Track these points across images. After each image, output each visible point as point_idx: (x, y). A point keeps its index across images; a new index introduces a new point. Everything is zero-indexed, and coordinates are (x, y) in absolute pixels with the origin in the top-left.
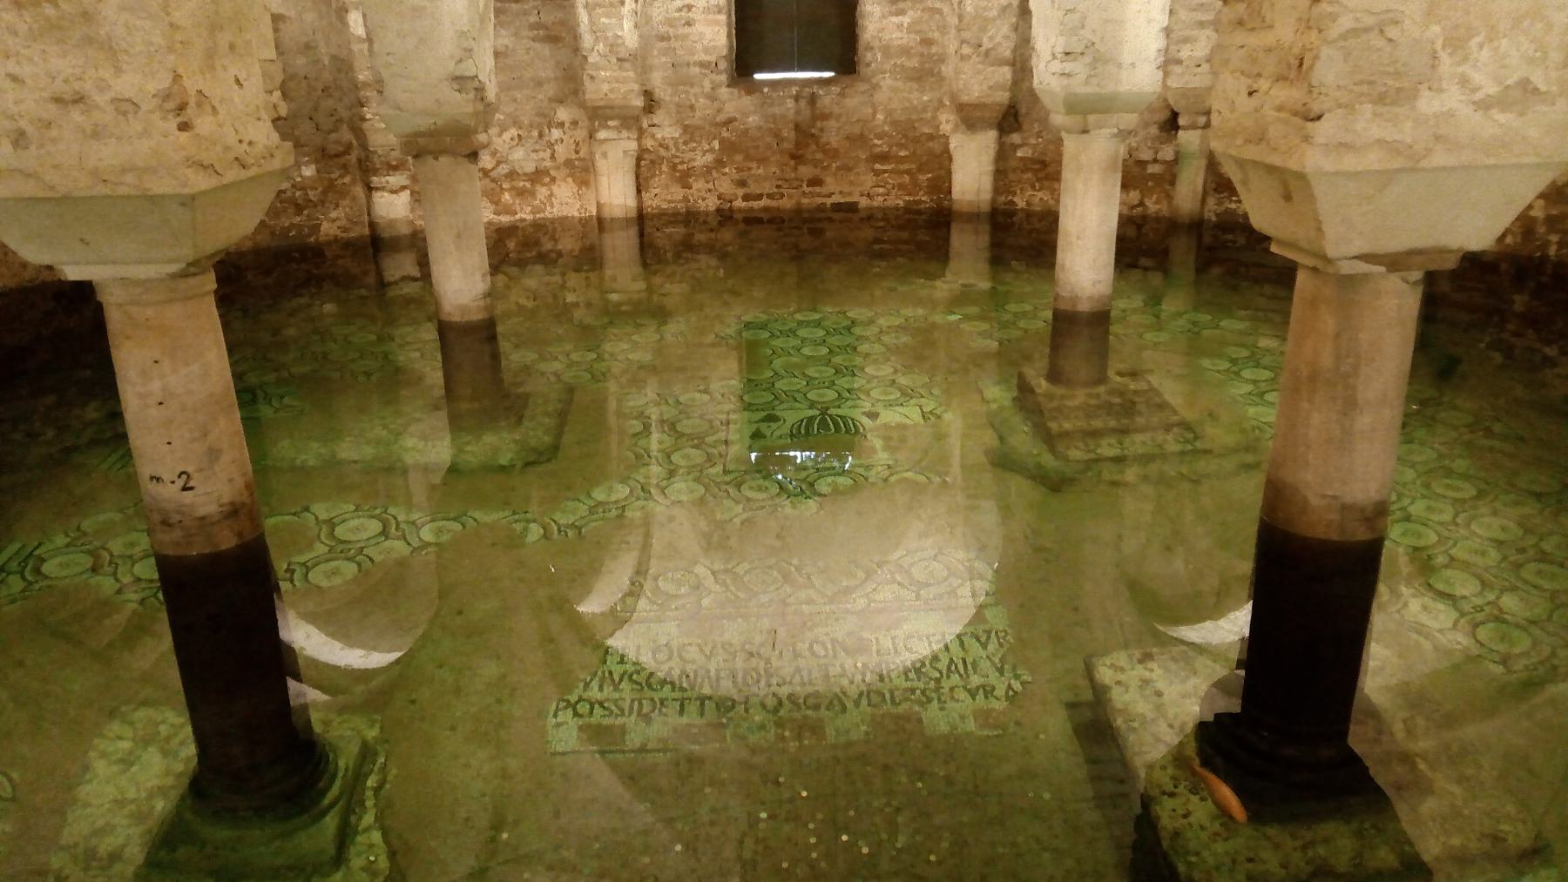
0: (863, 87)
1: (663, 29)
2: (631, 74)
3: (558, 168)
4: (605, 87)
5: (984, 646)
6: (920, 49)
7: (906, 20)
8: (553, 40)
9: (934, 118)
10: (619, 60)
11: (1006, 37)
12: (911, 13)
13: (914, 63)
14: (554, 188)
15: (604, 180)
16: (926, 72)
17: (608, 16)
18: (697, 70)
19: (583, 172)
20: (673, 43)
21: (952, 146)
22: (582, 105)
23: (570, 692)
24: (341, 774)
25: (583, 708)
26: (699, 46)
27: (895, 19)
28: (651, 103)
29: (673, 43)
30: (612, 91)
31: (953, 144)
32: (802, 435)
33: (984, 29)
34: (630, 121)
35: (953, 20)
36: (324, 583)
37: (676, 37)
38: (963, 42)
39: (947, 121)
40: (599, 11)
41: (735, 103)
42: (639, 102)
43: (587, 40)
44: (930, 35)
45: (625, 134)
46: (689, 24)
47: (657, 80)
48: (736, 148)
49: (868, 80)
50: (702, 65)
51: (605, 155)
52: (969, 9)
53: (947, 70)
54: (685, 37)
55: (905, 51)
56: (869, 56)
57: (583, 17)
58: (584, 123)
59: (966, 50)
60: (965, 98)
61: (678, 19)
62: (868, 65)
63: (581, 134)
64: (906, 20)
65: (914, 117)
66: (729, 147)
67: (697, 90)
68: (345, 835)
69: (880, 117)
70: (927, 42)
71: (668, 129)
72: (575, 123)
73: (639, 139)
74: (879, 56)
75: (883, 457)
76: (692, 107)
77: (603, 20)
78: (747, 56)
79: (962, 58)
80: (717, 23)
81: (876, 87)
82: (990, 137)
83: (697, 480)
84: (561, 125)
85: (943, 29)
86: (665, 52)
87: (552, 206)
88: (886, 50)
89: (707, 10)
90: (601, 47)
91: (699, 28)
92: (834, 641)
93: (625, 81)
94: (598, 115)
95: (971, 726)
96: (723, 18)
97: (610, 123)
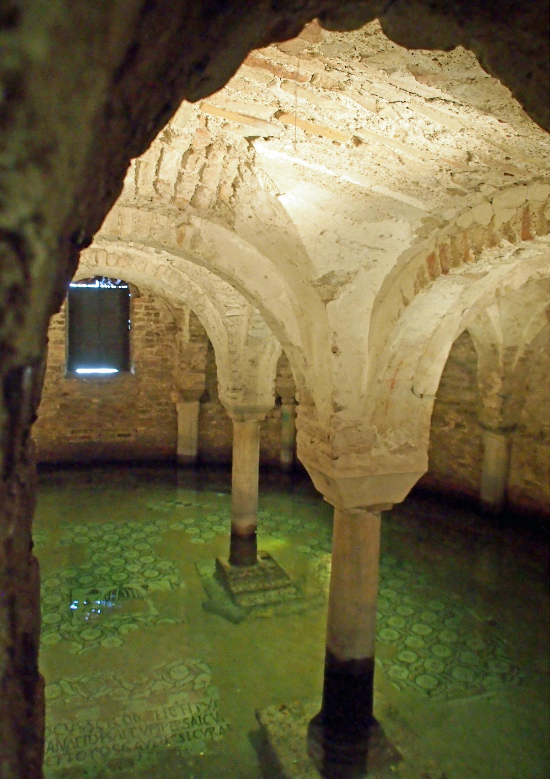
7: (154, 350)
11: (202, 361)
12: (157, 347)
13: (158, 369)
16: (165, 374)
21: (178, 409)
27: (149, 349)
35: (177, 351)
39: (174, 396)
44: (166, 357)
53: (175, 373)
55: (154, 363)
59: (184, 366)
60: (184, 387)
64: (154, 350)
66: (64, 407)
69: (142, 393)
70: (165, 360)
74: (141, 365)
79: (182, 369)
80: (60, 348)
82: (196, 404)
85: (172, 354)
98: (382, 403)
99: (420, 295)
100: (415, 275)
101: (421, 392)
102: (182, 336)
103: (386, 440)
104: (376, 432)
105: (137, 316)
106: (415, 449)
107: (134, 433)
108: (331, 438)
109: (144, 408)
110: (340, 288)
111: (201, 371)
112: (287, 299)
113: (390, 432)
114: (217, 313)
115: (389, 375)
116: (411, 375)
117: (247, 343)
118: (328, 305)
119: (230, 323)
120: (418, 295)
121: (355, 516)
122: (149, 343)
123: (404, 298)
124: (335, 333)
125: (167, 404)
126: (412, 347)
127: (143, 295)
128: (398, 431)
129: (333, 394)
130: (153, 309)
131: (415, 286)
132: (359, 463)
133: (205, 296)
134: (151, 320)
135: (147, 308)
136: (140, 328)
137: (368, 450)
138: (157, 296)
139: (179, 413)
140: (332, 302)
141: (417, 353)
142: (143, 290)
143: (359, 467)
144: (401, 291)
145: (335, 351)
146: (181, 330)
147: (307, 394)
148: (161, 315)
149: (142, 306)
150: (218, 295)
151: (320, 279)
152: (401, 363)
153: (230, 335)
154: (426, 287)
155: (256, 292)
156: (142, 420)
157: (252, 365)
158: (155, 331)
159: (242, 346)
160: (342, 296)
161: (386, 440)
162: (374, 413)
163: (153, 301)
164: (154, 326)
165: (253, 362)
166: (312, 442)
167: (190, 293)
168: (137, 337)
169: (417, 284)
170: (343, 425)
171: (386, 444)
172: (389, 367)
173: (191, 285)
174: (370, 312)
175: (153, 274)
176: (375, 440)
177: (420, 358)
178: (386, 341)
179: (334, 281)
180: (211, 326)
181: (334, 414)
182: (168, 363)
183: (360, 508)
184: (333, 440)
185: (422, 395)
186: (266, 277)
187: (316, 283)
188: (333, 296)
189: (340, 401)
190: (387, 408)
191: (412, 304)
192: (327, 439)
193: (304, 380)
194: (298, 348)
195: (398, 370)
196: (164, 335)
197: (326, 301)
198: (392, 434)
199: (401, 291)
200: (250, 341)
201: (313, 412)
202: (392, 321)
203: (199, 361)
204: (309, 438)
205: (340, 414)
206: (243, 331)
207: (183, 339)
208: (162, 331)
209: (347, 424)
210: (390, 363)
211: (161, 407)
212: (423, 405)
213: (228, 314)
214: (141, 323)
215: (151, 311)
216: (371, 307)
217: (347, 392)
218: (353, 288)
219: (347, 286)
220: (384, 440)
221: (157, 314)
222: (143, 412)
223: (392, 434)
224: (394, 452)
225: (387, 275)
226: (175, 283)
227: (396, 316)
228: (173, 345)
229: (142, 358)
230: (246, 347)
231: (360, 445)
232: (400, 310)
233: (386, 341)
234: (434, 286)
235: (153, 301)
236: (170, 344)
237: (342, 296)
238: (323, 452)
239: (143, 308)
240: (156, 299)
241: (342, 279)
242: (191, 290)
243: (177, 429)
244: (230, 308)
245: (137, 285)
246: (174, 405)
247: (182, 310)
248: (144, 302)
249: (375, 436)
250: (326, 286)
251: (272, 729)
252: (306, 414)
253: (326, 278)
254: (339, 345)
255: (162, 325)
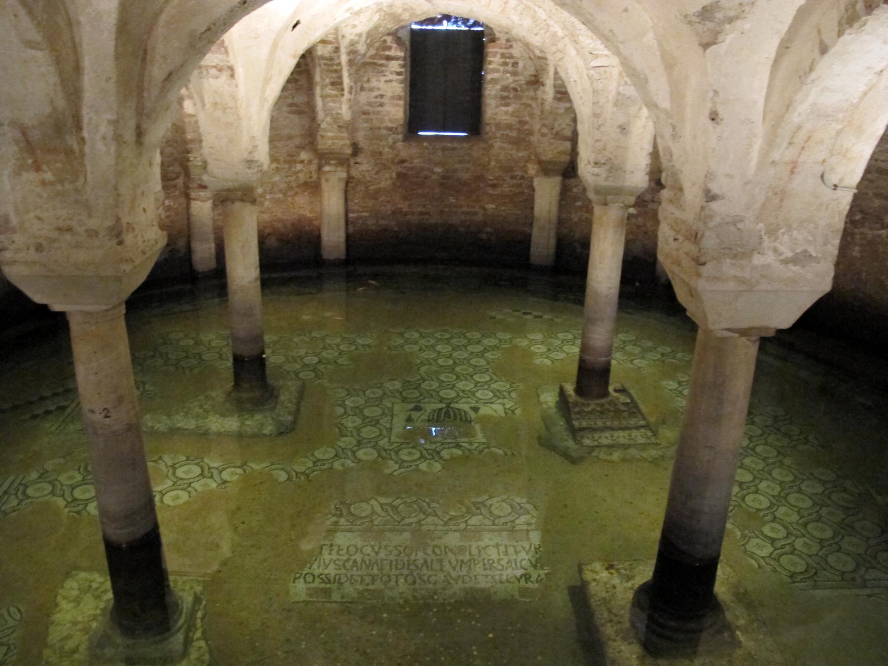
0: (482, 145)
1: (366, 108)
2: (346, 135)
3: (298, 187)
4: (330, 142)
5: (527, 553)
6: (517, 126)
7: (510, 109)
8: (300, 113)
9: (525, 166)
10: (339, 127)
12: (513, 105)
13: (514, 134)
14: (296, 198)
15: (325, 195)
17: (334, 102)
18: (384, 132)
19: (314, 188)
20: (372, 116)
22: (315, 151)
23: (303, 570)
24: (185, 611)
25: (309, 578)
26: (387, 118)
27: (503, 108)
28: (356, 149)
29: (372, 116)
30: (333, 144)
31: (536, 182)
32: (436, 418)
33: (555, 120)
34: (343, 162)
35: (537, 112)
36: (171, 503)
37: (374, 113)
38: (543, 125)
39: (532, 169)
40: (329, 99)
41: (406, 151)
42: (349, 151)
43: (321, 115)
45: (339, 169)
46: (381, 105)
47: (360, 137)
48: (408, 180)
49: (486, 143)
50: (389, 129)
51: (327, 180)
52: (547, 108)
53: (534, 139)
54: (379, 113)
55: (509, 127)
56: (488, 129)
57: (319, 102)
58: (315, 161)
59: (545, 130)
60: (543, 158)
61: (376, 102)
62: (487, 133)
63: (314, 167)
64: (510, 109)
65: (513, 165)
66: (401, 176)
67: (384, 143)
68: (188, 642)
69: (493, 163)
70: (522, 123)
71: (366, 165)
72: (310, 162)
73: (348, 172)
74: (494, 129)
75: (480, 437)
76: (380, 153)
77: (332, 104)
78: (415, 121)
79: (543, 135)
80: (398, 105)
81: (492, 146)
83: (374, 447)
84: (302, 162)
85: (532, 115)
86: (367, 121)
87: (294, 208)
88: (498, 126)
89: (393, 98)
90: (328, 119)
91: (387, 108)
92: (445, 547)
93: (342, 138)
94: (323, 157)
95: (517, 595)
96: (402, 102)
97: (332, 162)
98: (776, 194)
99: (846, 37)
100: (842, 8)
101: (835, 182)
102: (544, 92)
103: (776, 244)
104: (763, 233)
105: (490, 67)
106: (816, 260)
107: (481, 212)
108: (699, 236)
109: (495, 182)
110: (727, 26)
111: (566, 139)
112: (655, 41)
113: (783, 234)
114: (581, 63)
115: (789, 155)
116: (821, 157)
117: (616, 104)
118: (707, 51)
119: (596, 76)
120: (842, 39)
121: (723, 340)
122: (504, 100)
123: (821, 42)
124: (715, 92)
125: (522, 177)
126: (828, 116)
127: (499, 39)
128: (795, 233)
129: (706, 176)
130: (511, 57)
131: (840, 24)
132: (732, 272)
133: (567, 39)
134: (507, 72)
135: (503, 56)
136: (495, 81)
137: (747, 255)
138: (515, 40)
139: (537, 188)
140: (715, 46)
141: (834, 125)
142: (500, 32)
143: (735, 276)
144: (819, 32)
145: (714, 117)
146: (543, 84)
147: (675, 175)
148: (521, 65)
149: (497, 52)
150: (581, 39)
151: (698, 12)
152: (809, 138)
153: (595, 92)
154: (856, 25)
155: (611, 31)
156: (491, 195)
157: (621, 133)
158: (512, 86)
159: (610, 108)
160: (729, 38)
161: (776, 244)
162: (763, 206)
163: (511, 46)
164: (511, 79)
165: (623, 129)
166: (675, 240)
167: (547, 35)
168: (491, 92)
169: (844, 21)
170: (717, 220)
171: (775, 250)
172: (790, 144)
173: (548, 25)
174: (771, 63)
175: (500, 10)
176: (760, 243)
177: (839, 133)
178: (788, 106)
179: (719, 16)
180: (572, 80)
181: (705, 204)
182: (526, 127)
183: (729, 330)
184: (701, 239)
185: (835, 186)
186: (626, 10)
187: (694, 19)
188: (716, 39)
189: (715, 188)
190: (781, 200)
191: (832, 51)
192: (695, 237)
193: (671, 156)
194: (666, 110)
195: (803, 148)
196: (522, 91)
197: (706, 46)
198: (786, 237)
199: (819, 32)
200: (621, 101)
201: (680, 199)
202: (800, 77)
203: (564, 126)
204: (672, 233)
205: (715, 205)
206: (612, 87)
207: (545, 97)
208: (520, 86)
209: (722, 219)
210: (792, 138)
211: (515, 181)
212: (836, 199)
213: (594, 64)
214: (495, 75)
215: (508, 60)
216: (773, 55)
217: (727, 175)
218: (747, 26)
219: (738, 23)
220: (773, 244)
221: (515, 64)
222: (494, 186)
223: (786, 237)
224: (786, 262)
225: (801, 7)
226: (527, 22)
227: (808, 70)
228: (534, 105)
229: (495, 119)
230: (615, 109)
231: (739, 249)
232: (814, 60)
233: (788, 106)
234: (869, 23)
235: (511, 46)
236: (529, 102)
237: (730, 38)
238: (687, 254)
239: (499, 56)
240: (514, 44)
241: (732, 13)
242: (547, 31)
243: (532, 208)
244: (596, 57)
245: (492, 26)
246: (531, 179)
247: (545, 59)
248: (501, 48)
249: (761, 238)
250: (707, 23)
251: (593, 588)
252: (671, 201)
253: (707, 11)
254: (721, 110)
255: (521, 78)
